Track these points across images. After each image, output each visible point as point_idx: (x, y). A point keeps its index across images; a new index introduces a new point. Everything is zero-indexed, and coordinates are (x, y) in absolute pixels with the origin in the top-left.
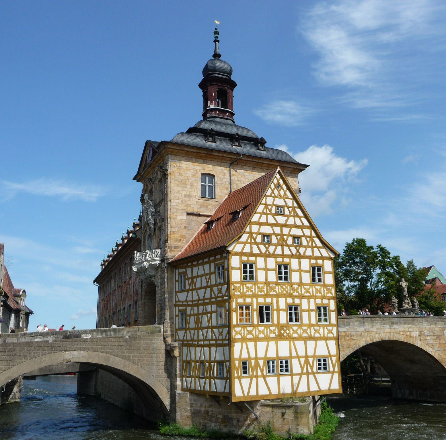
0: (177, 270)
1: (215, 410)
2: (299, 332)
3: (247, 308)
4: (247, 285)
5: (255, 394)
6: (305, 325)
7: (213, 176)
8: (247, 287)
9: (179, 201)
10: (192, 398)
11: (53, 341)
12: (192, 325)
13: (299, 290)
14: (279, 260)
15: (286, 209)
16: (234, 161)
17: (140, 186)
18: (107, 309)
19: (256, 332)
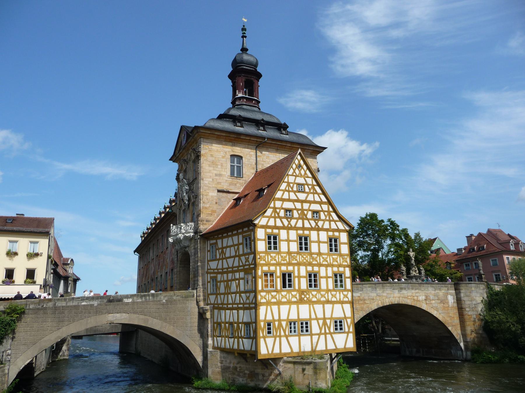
1: (242, 366)
2: (317, 296)
3: (272, 275)
4: (271, 255)
5: (278, 351)
6: (323, 290)
7: (241, 157)
8: (271, 257)
9: (211, 180)
10: (222, 355)
11: (98, 305)
12: (222, 290)
13: (318, 259)
14: (300, 232)
15: (306, 186)
16: (260, 143)
17: (176, 166)
18: (146, 275)
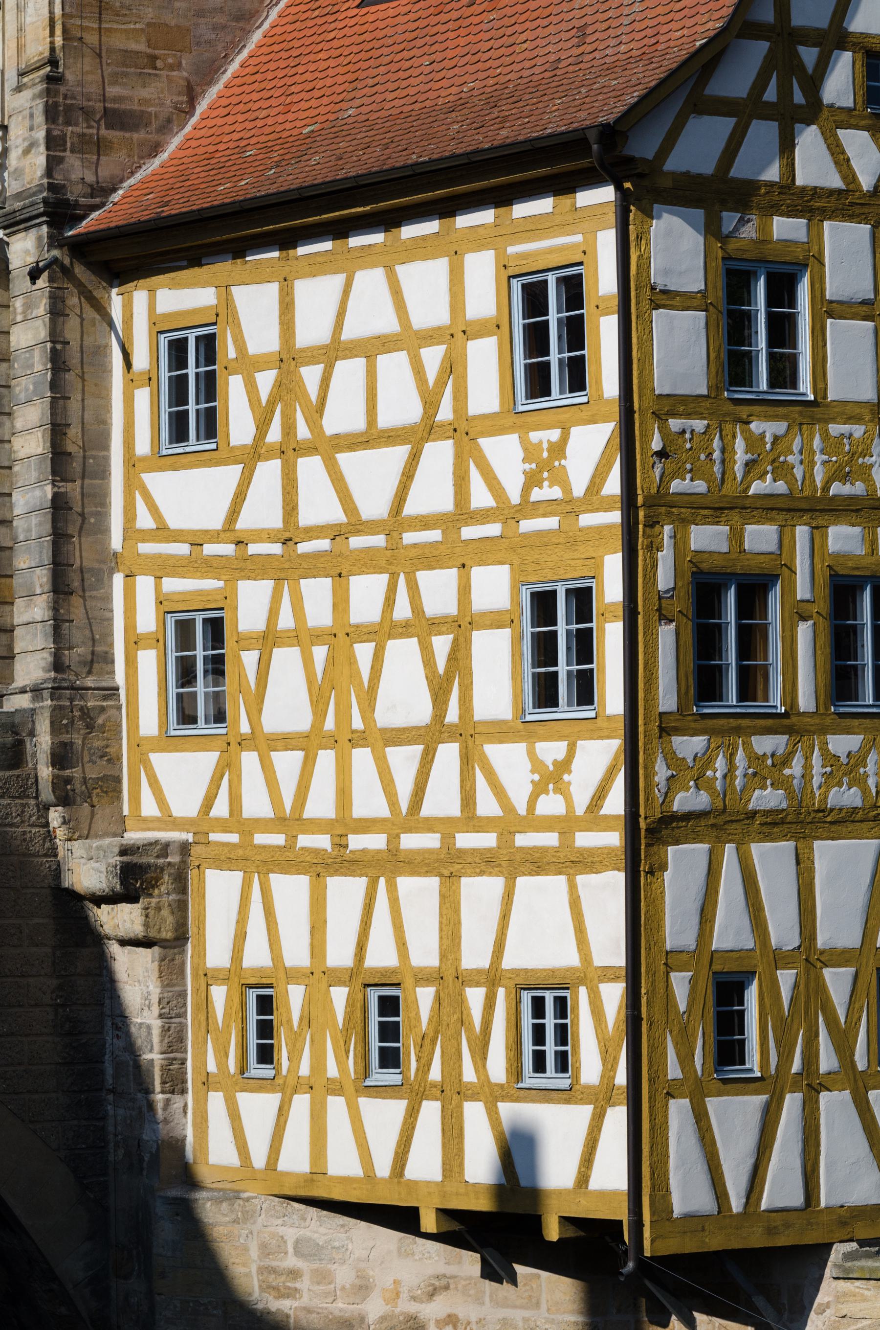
0: (140, 297)
1: (467, 1311)
5: (796, 1199)
8: (754, 443)
19: (807, 766)
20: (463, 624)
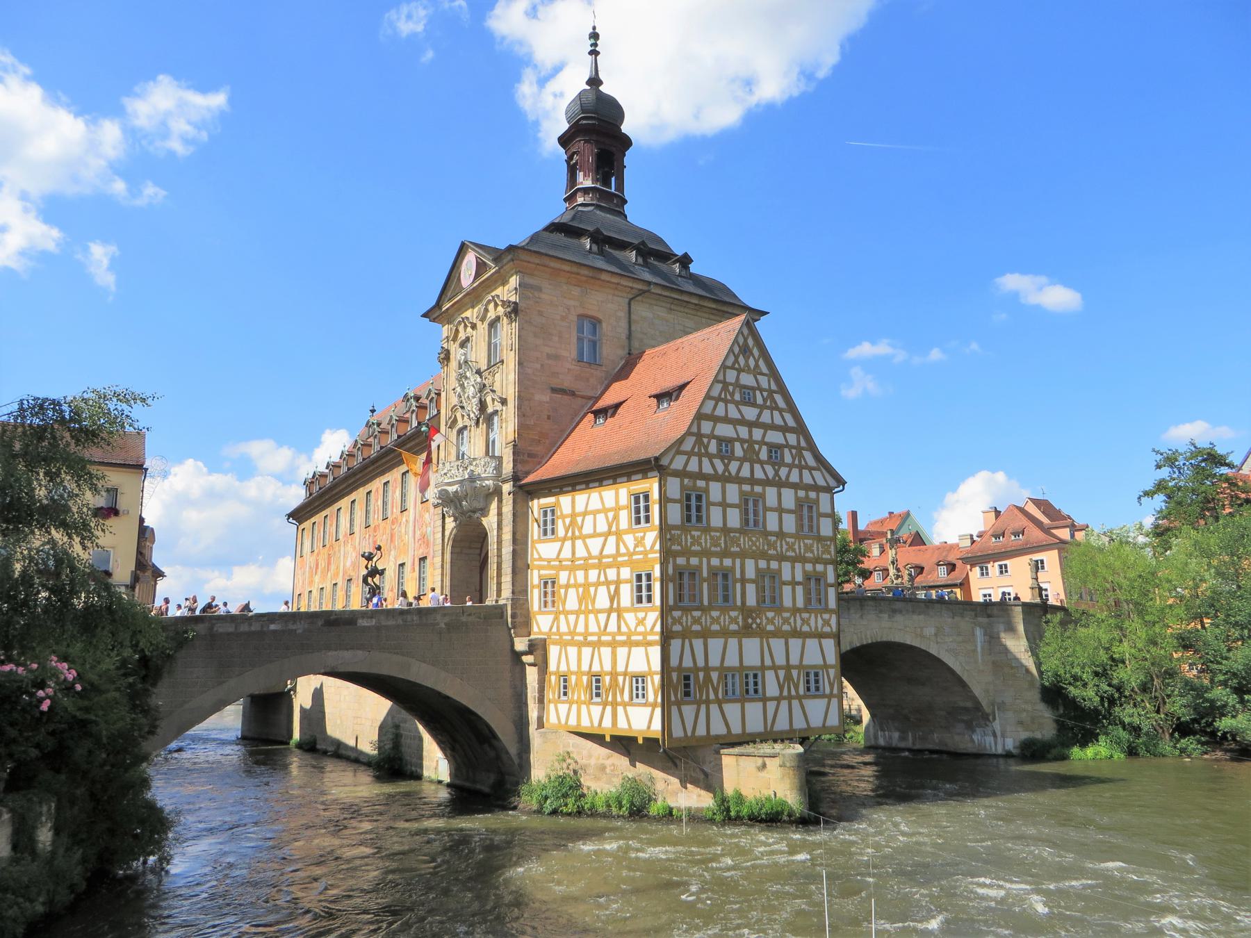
0: (536, 501)
3: (692, 575)
5: (704, 733)
6: (787, 610)
8: (692, 537)
10: (571, 742)
15: (758, 392)
20: (618, 583)
